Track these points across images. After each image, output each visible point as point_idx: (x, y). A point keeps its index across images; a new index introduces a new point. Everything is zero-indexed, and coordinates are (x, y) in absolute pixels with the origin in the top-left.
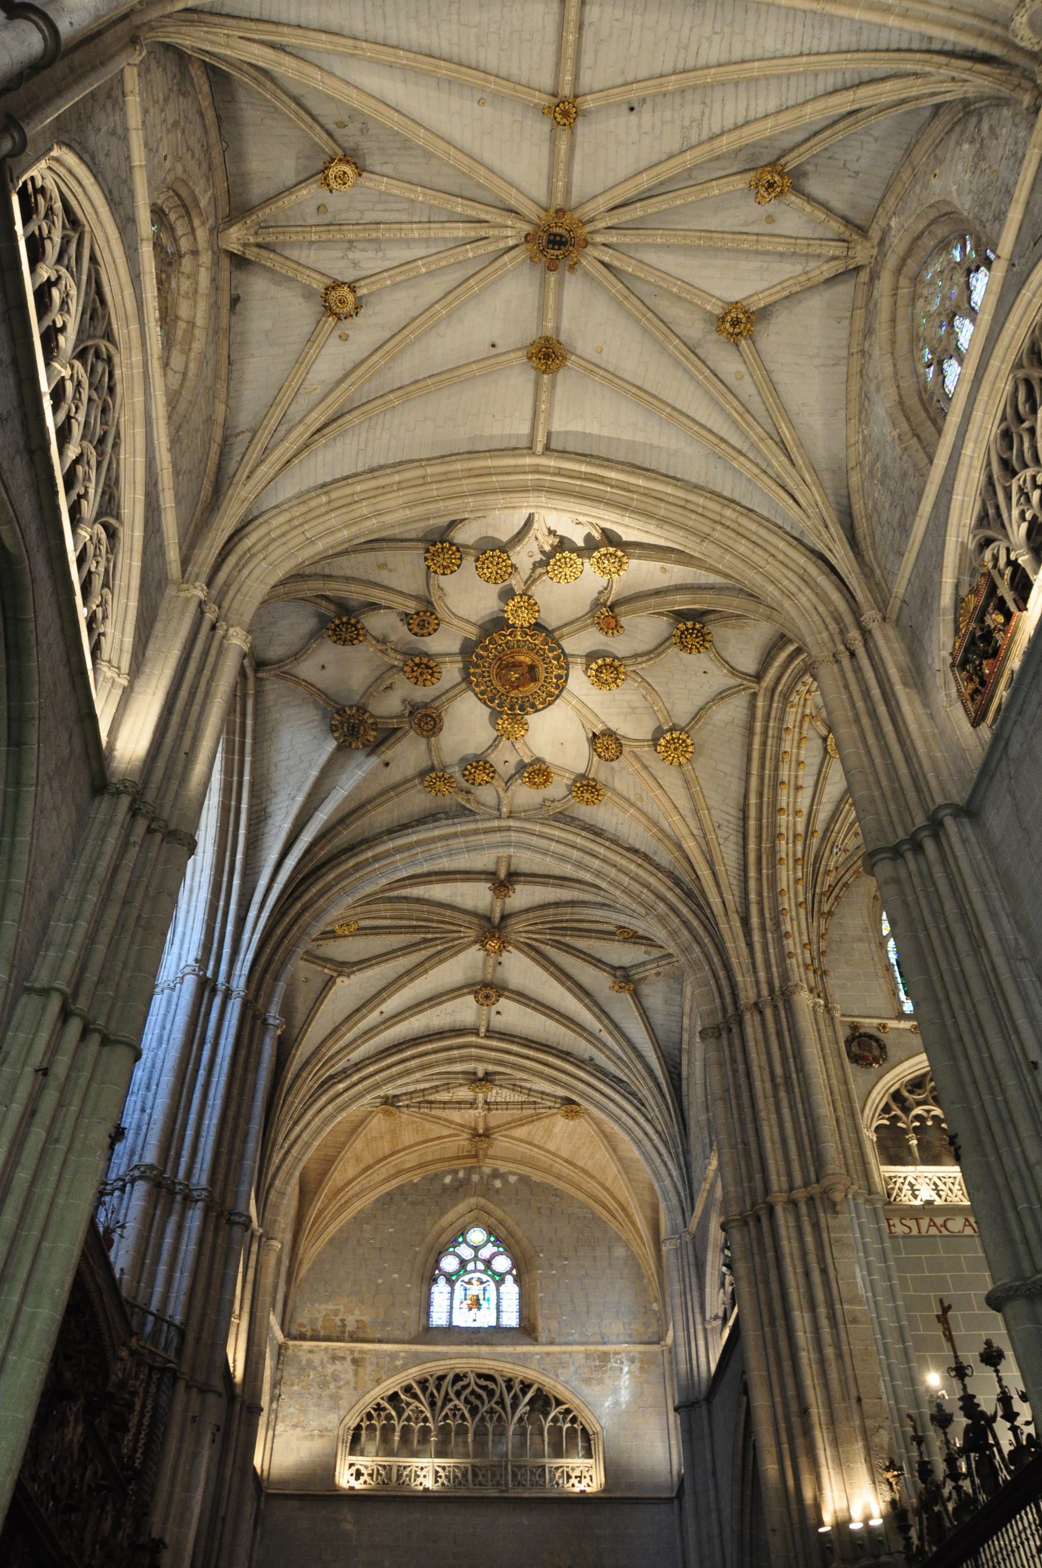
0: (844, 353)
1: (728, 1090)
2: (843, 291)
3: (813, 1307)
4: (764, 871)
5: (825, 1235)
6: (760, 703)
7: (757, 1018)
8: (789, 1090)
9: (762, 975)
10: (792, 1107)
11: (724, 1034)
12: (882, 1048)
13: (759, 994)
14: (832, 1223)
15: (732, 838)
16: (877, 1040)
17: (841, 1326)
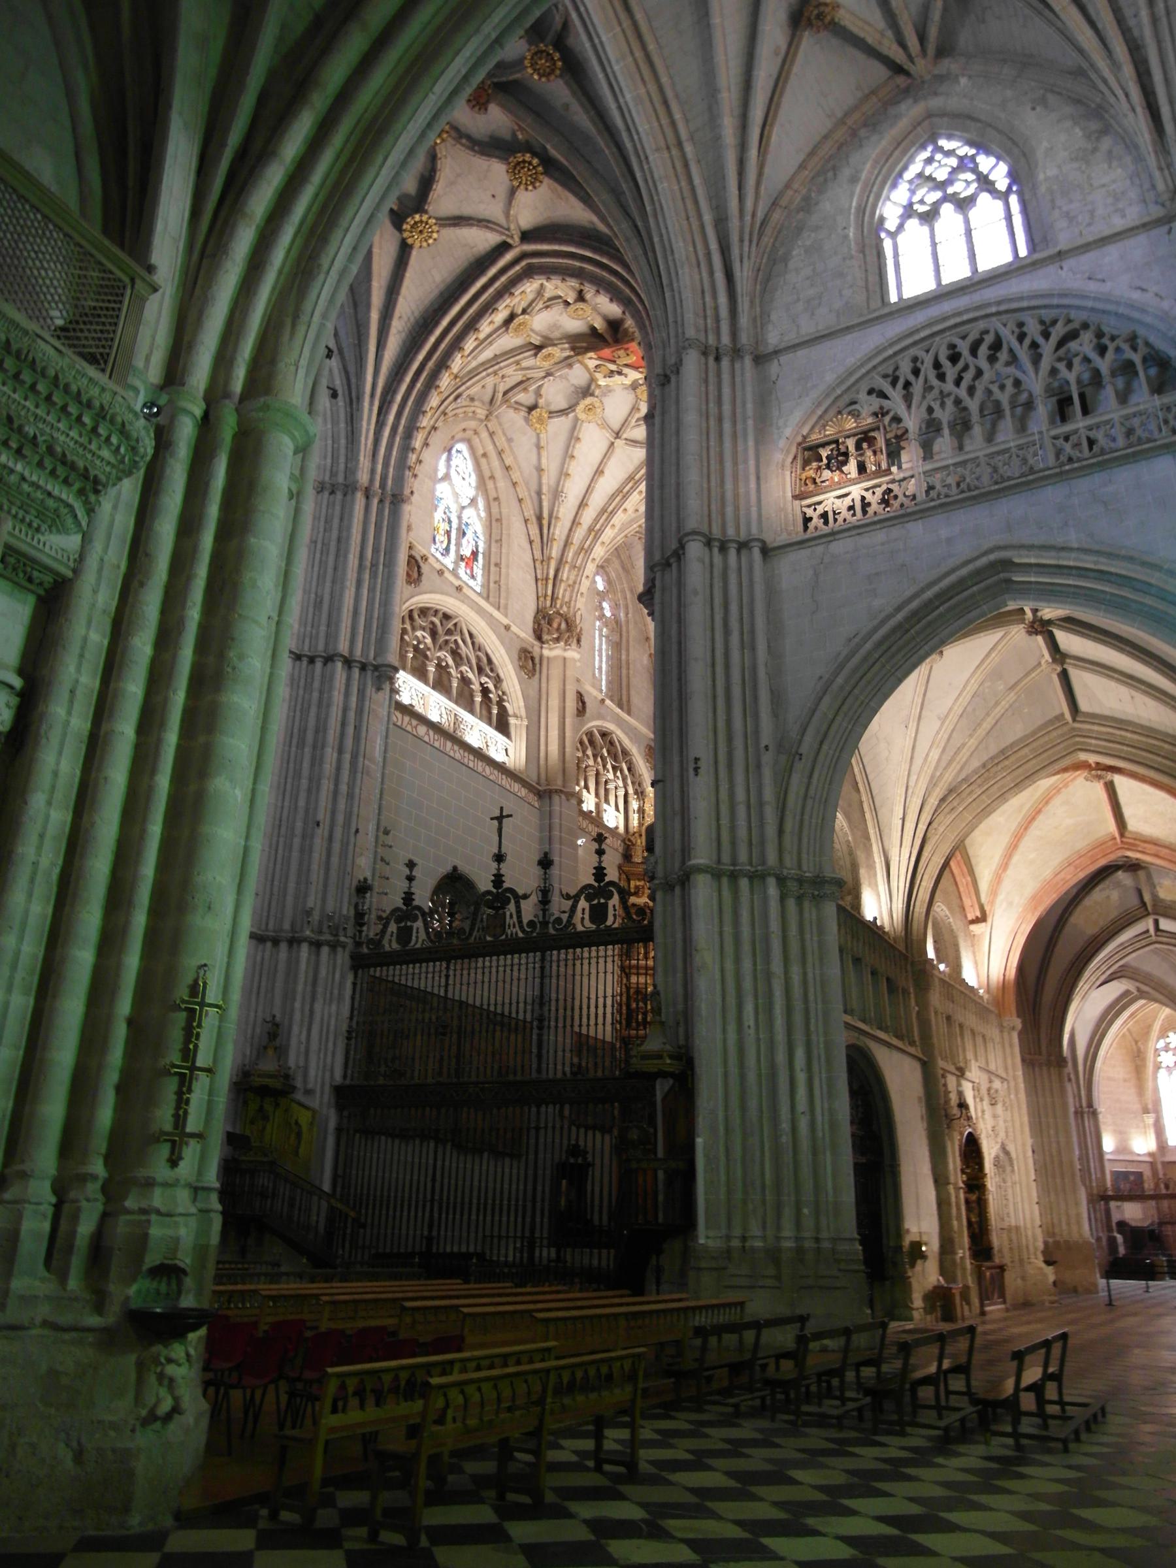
0: (839, 114)
1: (316, 542)
2: (880, 72)
3: (340, 751)
4: (418, 385)
5: (367, 703)
6: (509, 257)
7: (363, 501)
8: (373, 575)
9: (379, 467)
10: (372, 590)
11: (326, 494)
12: (420, 574)
13: (372, 480)
14: (374, 696)
15: (403, 335)
16: (419, 567)
17: (359, 775)
